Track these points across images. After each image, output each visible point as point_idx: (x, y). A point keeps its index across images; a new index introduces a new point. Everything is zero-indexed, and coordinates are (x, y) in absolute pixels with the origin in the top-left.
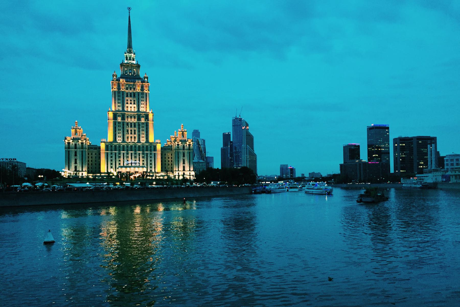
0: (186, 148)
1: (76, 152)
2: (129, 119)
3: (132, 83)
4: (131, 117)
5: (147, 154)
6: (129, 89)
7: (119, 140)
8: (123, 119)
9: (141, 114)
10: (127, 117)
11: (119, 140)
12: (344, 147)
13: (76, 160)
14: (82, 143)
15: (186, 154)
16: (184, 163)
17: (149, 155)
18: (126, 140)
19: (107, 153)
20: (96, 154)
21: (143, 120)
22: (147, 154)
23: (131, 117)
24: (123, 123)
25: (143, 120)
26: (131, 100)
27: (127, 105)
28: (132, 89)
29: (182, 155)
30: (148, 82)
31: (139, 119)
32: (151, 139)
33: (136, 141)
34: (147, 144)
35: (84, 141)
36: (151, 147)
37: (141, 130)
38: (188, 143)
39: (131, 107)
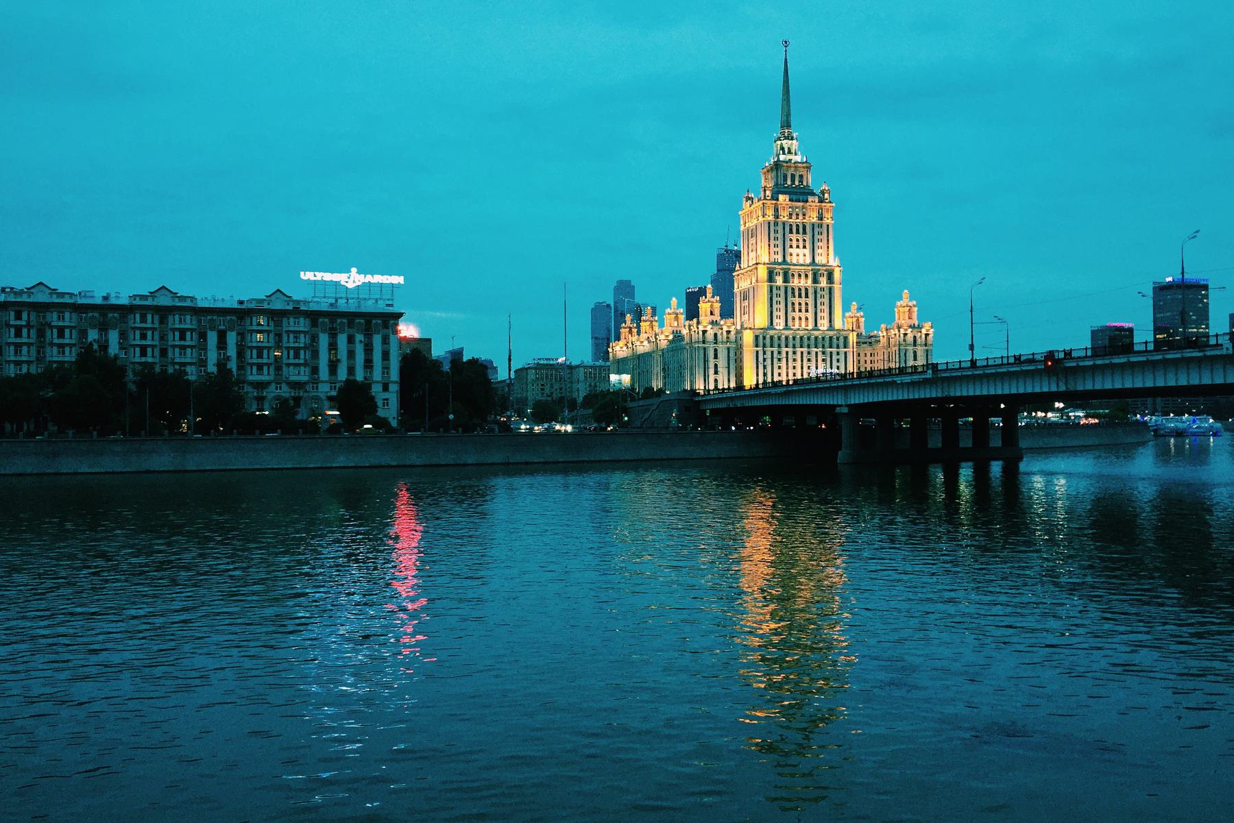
2: (796, 280)
3: (801, 204)
6: (794, 216)
7: (779, 324)
8: (786, 280)
11: (779, 324)
12: (1093, 332)
15: (919, 354)
17: (835, 357)
21: (823, 282)
25: (823, 282)
28: (801, 217)
32: (838, 324)
33: (810, 327)
34: (831, 333)
38: (924, 331)
39: (799, 256)
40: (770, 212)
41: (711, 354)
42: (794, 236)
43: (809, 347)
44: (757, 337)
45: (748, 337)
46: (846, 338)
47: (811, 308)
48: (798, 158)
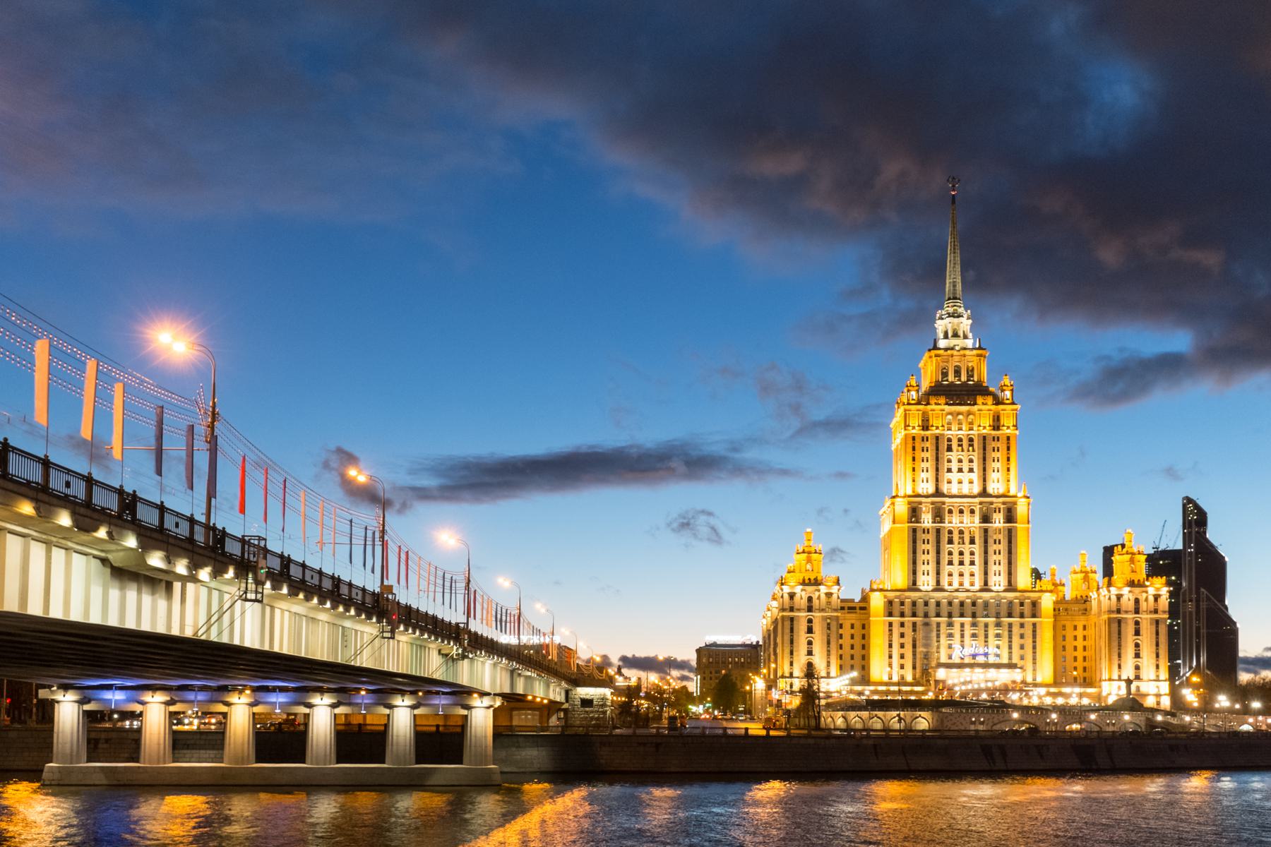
0: (1143, 606)
1: (810, 621)
4: (961, 512)
5: (1010, 625)
6: (954, 427)
9: (992, 503)
10: (950, 512)
11: (926, 582)
13: (810, 643)
14: (829, 595)
16: (1137, 656)
17: (1016, 630)
18: (945, 581)
19: (891, 624)
20: (852, 627)
21: (998, 521)
22: (1010, 625)
23: (961, 512)
24: (938, 531)
25: (998, 521)
26: (960, 461)
27: (948, 476)
30: (1013, 403)
32: (1023, 579)
33: (977, 587)
35: (835, 589)
36: (1022, 604)
37: (991, 551)
40: (915, 422)
41: (802, 627)
43: (974, 615)
44: (890, 603)
45: (877, 602)
46: (1035, 604)
47: (978, 558)
48: (969, 343)
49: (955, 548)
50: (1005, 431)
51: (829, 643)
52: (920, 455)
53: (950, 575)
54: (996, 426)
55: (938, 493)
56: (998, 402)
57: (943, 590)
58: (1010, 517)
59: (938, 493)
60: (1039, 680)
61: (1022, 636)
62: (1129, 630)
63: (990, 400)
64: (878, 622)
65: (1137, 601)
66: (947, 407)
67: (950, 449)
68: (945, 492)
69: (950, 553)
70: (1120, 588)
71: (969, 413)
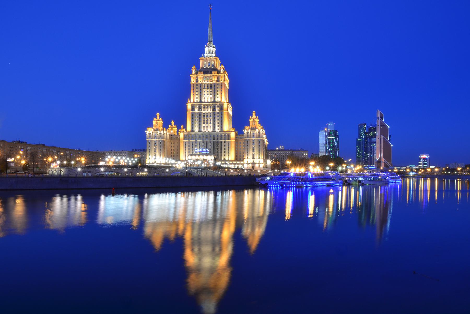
0: (255, 135)
4: (207, 107)
8: (200, 109)
10: (204, 107)
11: (196, 129)
14: (160, 133)
17: (223, 144)
21: (218, 110)
23: (207, 107)
24: (200, 114)
25: (218, 110)
29: (251, 143)
31: (214, 109)
42: (206, 90)
49: (205, 118)
50: (221, 82)
51: (185, 149)
52: (195, 90)
53: (204, 127)
54: (218, 80)
55: (201, 101)
56: (219, 72)
57: (201, 132)
58: (221, 108)
59: (201, 101)
60: (230, 159)
61: (225, 146)
62: (251, 143)
63: (216, 72)
64: (182, 141)
65: (253, 133)
66: (203, 75)
67: (204, 88)
68: (203, 101)
69: (204, 120)
70: (247, 130)
71: (210, 77)
